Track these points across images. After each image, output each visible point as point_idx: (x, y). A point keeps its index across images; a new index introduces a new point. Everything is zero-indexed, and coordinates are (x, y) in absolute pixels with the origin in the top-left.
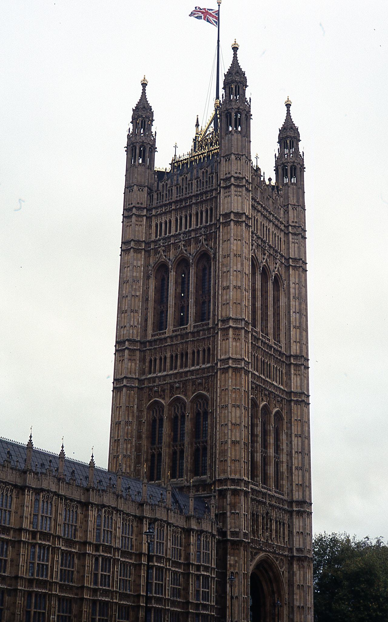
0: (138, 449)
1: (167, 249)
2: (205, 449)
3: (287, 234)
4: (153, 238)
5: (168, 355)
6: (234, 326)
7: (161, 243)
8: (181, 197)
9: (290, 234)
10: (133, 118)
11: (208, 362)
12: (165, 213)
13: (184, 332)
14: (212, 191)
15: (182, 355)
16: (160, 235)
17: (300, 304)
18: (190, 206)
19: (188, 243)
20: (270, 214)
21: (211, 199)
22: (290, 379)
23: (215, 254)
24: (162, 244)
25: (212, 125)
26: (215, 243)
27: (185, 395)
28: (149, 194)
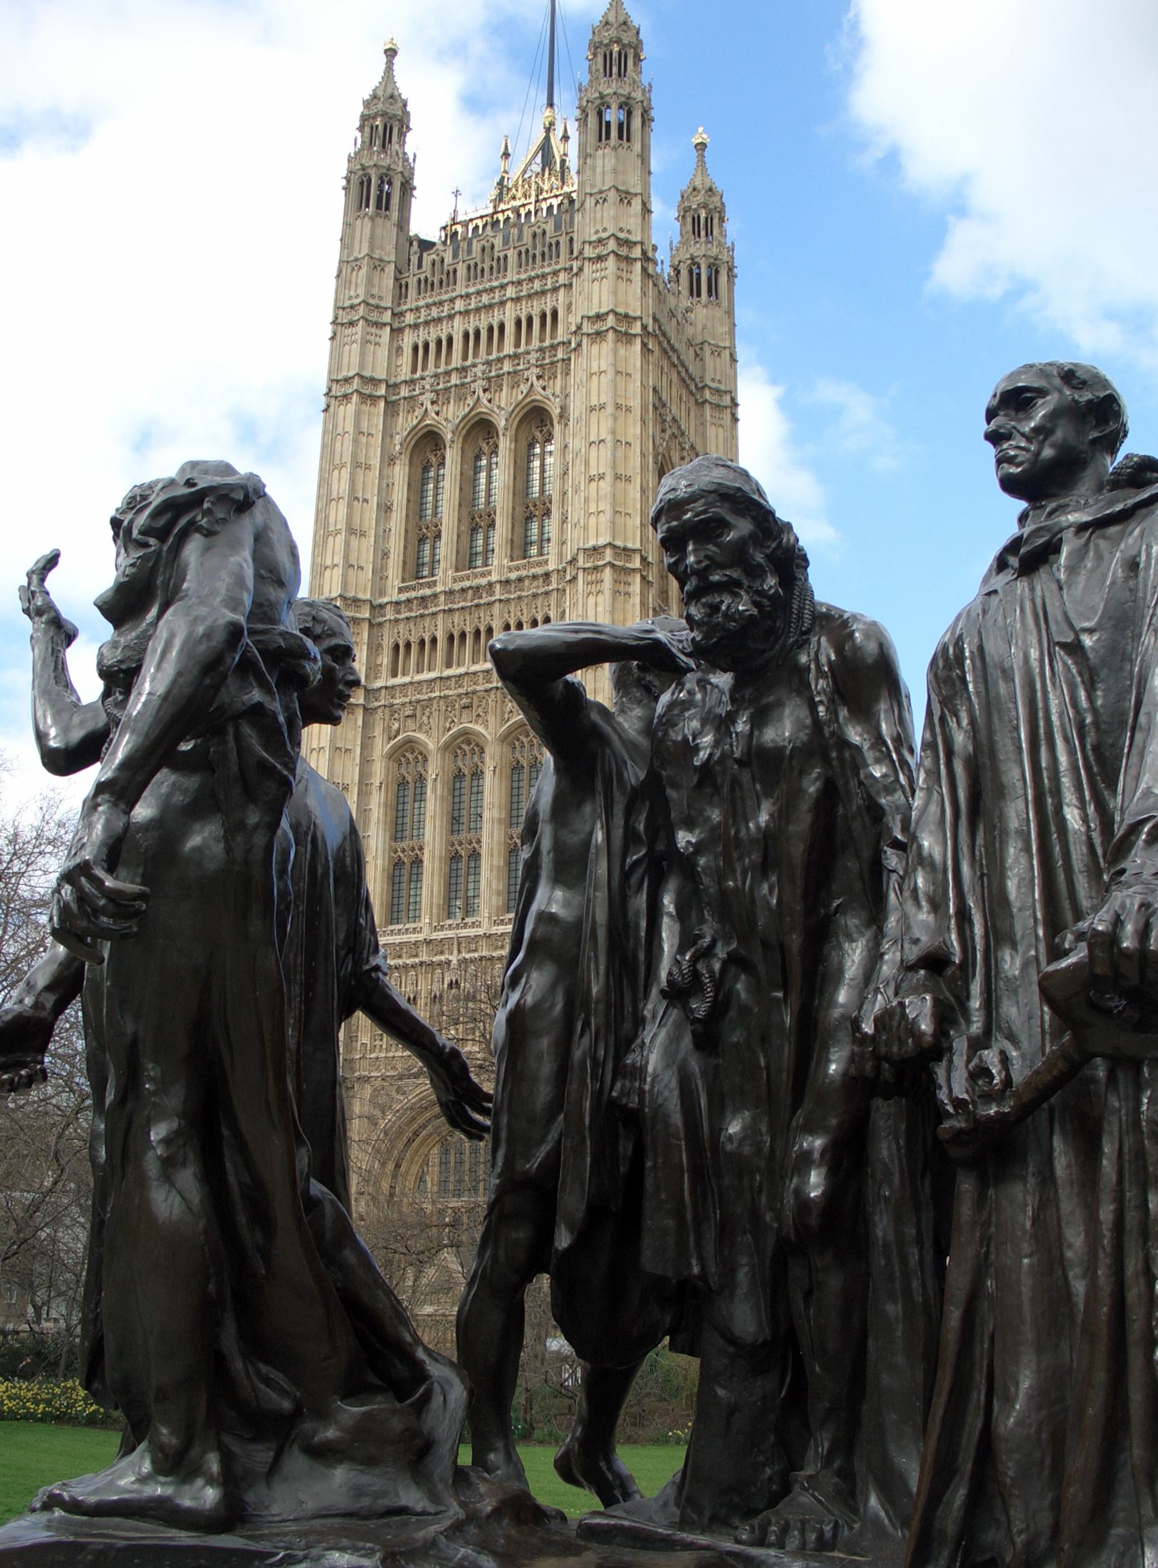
4: (405, 373)
9: (707, 407)
10: (364, 118)
14: (555, 273)
18: (502, 303)
19: (493, 384)
23: (564, 409)
24: (428, 387)
25: (539, 159)
28: (396, 279)
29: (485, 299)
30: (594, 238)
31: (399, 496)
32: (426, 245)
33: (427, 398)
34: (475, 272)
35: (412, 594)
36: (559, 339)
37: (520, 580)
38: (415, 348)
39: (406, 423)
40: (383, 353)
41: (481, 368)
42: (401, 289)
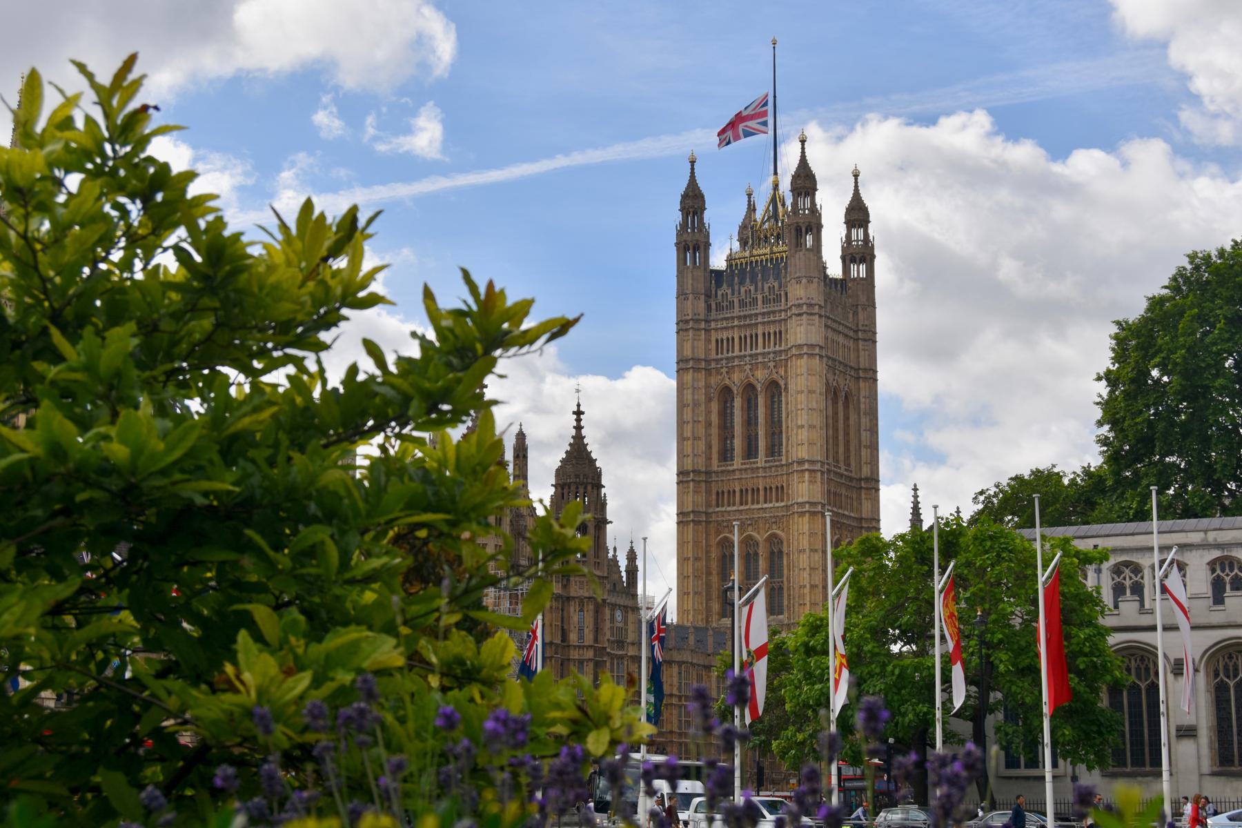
0: (708, 586)
1: (730, 370)
2: (781, 589)
3: (857, 340)
4: (713, 355)
5: (737, 489)
6: (811, 468)
7: (724, 362)
8: (746, 313)
11: (782, 501)
12: (726, 328)
13: (755, 466)
15: (753, 490)
16: (722, 353)
17: (871, 420)
20: (840, 323)
21: (780, 321)
22: (861, 504)
23: (786, 384)
25: (771, 208)
26: (786, 371)
27: (759, 533)
29: (748, 322)
30: (797, 302)
31: (715, 418)
32: (718, 274)
33: (724, 370)
34: (742, 304)
35: (723, 468)
36: (782, 348)
37: (770, 467)
38: (717, 341)
39: (714, 380)
40: (701, 344)
41: (748, 358)
42: (709, 308)
